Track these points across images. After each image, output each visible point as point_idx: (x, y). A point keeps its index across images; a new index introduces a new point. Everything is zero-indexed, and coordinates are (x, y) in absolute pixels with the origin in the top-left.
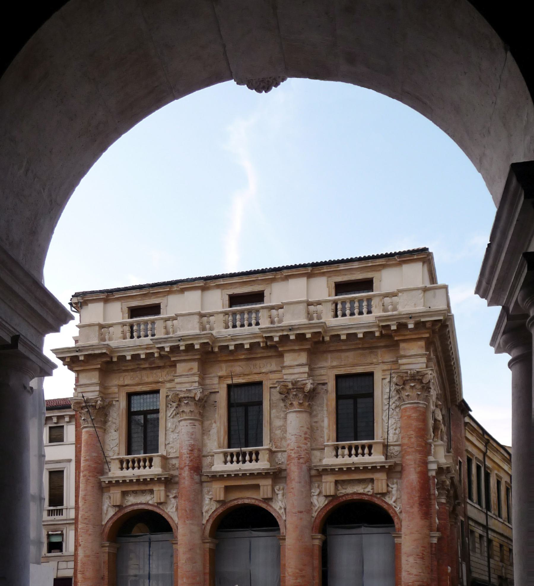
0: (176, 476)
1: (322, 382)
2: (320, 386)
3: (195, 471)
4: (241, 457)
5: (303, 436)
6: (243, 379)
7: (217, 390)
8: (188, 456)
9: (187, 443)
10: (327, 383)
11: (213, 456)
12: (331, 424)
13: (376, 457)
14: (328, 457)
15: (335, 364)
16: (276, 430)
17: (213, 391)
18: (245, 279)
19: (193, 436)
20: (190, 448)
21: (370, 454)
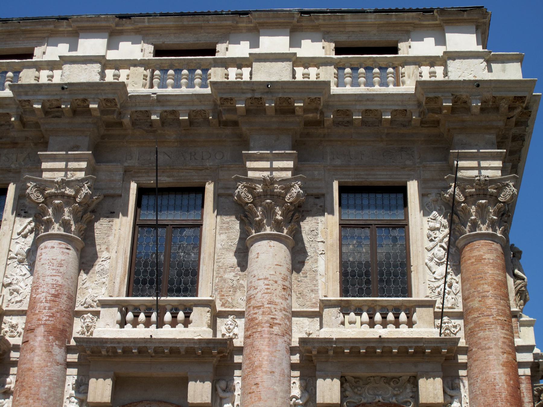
0: (16, 348)
1: (315, 192)
2: (311, 200)
3: (57, 338)
4: (155, 314)
5: (280, 282)
6: (169, 177)
7: (118, 192)
8: (48, 305)
9: (49, 280)
10: (323, 195)
11: (97, 314)
12: (330, 267)
13: (423, 330)
14: (329, 326)
15: (338, 162)
16: (225, 272)
17: (111, 192)
18: (186, 21)
19: (62, 269)
20: (53, 291)
21: (410, 324)
